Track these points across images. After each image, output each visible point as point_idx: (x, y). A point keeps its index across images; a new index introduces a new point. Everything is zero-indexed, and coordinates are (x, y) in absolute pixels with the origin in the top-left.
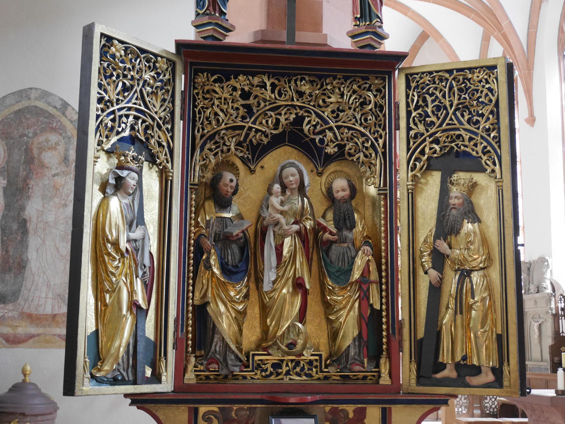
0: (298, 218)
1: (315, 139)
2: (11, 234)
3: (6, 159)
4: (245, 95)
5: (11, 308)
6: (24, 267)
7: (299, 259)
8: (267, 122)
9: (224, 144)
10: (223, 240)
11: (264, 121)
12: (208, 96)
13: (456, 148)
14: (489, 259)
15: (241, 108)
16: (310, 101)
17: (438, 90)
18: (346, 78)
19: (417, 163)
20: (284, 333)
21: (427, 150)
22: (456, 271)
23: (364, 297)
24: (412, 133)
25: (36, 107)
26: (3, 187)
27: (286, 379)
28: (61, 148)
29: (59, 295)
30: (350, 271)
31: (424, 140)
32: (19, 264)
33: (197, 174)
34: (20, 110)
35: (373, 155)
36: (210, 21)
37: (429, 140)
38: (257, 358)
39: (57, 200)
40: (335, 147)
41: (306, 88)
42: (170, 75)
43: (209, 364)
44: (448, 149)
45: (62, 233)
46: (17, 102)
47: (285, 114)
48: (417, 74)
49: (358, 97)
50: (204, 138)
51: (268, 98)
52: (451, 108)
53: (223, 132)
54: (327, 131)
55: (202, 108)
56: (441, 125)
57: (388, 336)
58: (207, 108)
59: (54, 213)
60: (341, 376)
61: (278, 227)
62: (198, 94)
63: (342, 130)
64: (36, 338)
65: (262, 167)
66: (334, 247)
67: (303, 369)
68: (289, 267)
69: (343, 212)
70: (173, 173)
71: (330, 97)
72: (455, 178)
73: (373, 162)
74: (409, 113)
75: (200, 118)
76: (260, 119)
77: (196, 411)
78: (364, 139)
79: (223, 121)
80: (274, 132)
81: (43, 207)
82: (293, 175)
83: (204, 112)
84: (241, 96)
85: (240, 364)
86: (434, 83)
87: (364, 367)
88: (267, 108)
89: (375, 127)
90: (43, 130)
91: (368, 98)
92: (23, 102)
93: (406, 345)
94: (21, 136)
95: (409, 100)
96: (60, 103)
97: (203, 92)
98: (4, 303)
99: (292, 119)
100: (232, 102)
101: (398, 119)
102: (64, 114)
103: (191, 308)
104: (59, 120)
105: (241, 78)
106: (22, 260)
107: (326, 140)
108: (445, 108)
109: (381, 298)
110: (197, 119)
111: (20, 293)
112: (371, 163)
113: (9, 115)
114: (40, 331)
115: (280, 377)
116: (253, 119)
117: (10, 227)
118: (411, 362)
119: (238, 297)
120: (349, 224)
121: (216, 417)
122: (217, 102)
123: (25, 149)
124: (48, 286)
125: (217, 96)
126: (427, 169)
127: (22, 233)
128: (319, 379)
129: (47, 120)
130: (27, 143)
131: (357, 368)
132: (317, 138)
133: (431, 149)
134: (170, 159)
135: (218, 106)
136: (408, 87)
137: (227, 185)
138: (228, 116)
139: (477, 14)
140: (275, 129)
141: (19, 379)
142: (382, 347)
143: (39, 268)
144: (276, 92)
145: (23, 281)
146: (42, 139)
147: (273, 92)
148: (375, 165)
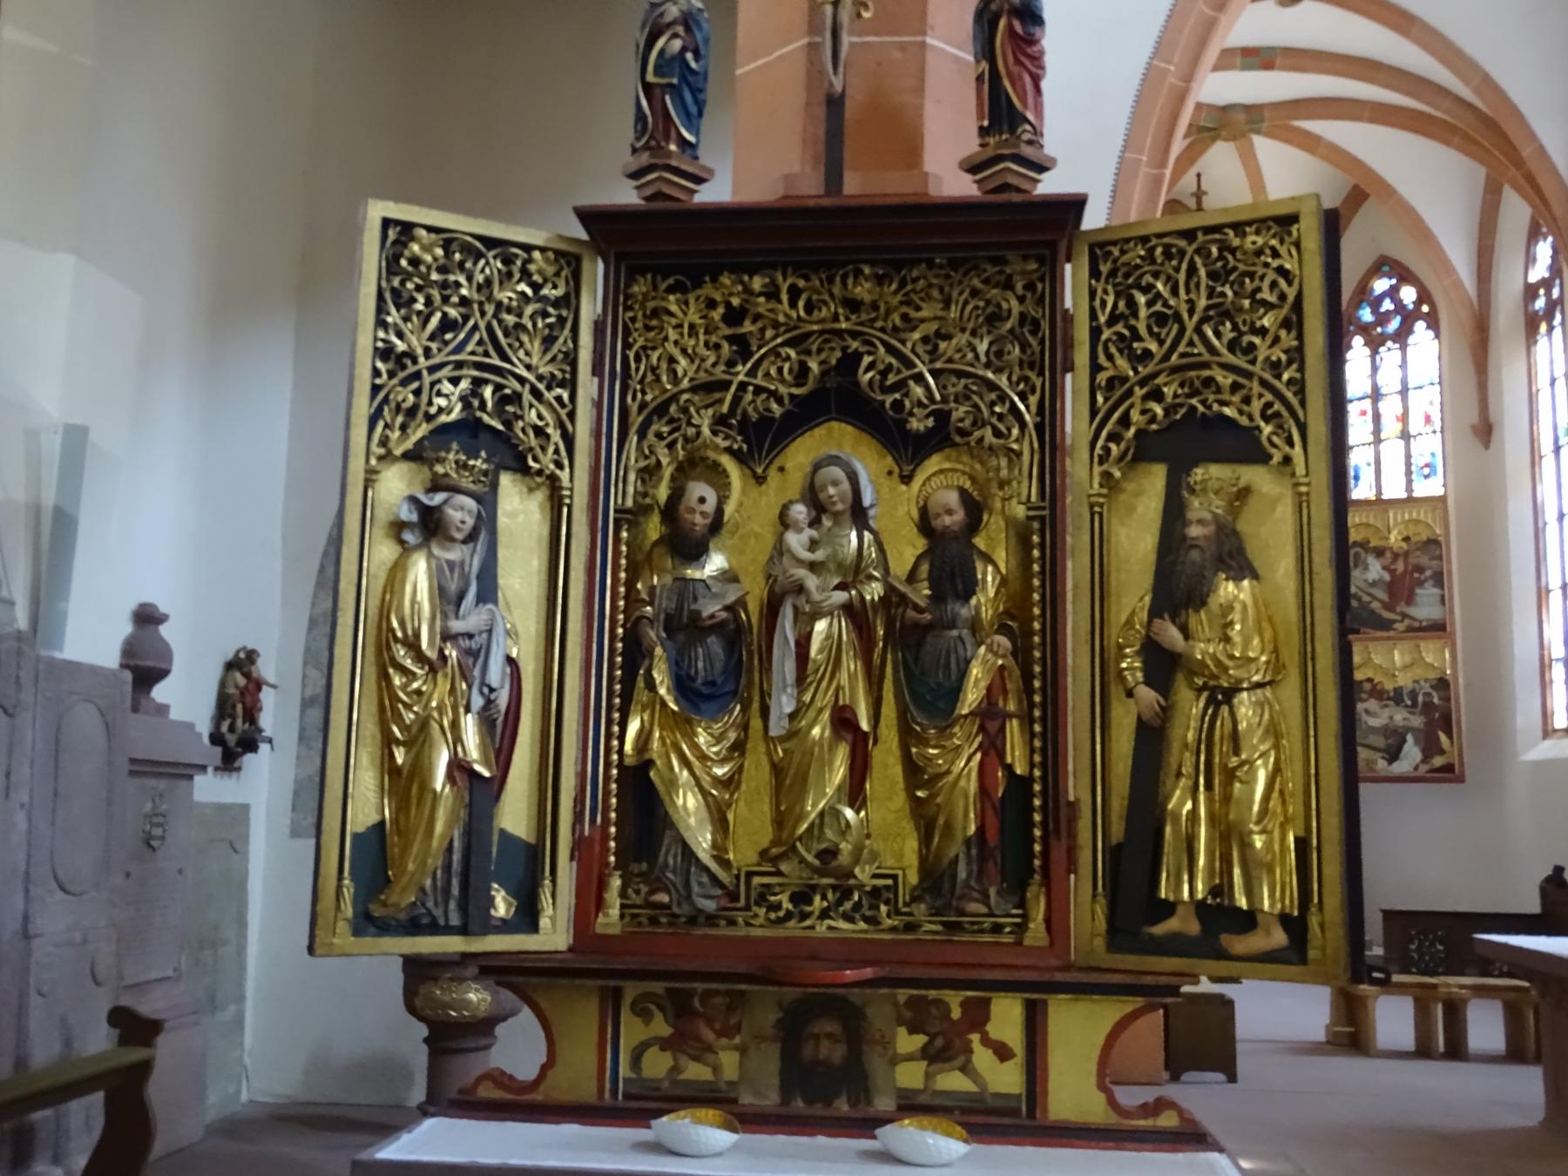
0: (850, 579)
1: (883, 402)
4: (734, 316)
7: (851, 664)
8: (780, 370)
9: (689, 424)
10: (684, 626)
11: (773, 371)
12: (654, 323)
13: (1201, 408)
14: (1276, 665)
15: (726, 346)
16: (874, 320)
17: (1163, 277)
18: (954, 264)
19: (1113, 447)
20: (812, 825)
21: (1135, 416)
22: (1200, 690)
23: (993, 748)
24: (1102, 378)
27: (821, 929)
30: (956, 692)
31: (1130, 393)
33: (631, 490)
35: (1015, 432)
36: (653, 161)
37: (1139, 392)
38: (757, 880)
40: (927, 416)
41: (863, 290)
42: (567, 283)
43: (653, 892)
44: (1183, 411)
47: (820, 351)
48: (1114, 243)
49: (982, 304)
50: (646, 412)
51: (781, 319)
52: (1191, 316)
53: (685, 396)
54: (911, 383)
55: (644, 348)
56: (1166, 358)
57: (1045, 840)
58: (654, 349)
60: (942, 923)
61: (803, 598)
62: (633, 320)
63: (942, 380)
65: (781, 469)
66: (929, 639)
67: (857, 906)
68: (824, 684)
69: (949, 558)
70: (571, 489)
71: (918, 309)
72: (1199, 478)
73: (1015, 446)
74: (1095, 332)
75: (637, 369)
76: (765, 364)
77: (617, 995)
78: (993, 396)
79: (685, 374)
80: (795, 391)
82: (835, 483)
83: (648, 357)
84: (725, 318)
85: (719, 892)
86: (1153, 261)
87: (988, 906)
88: (779, 340)
89: (1021, 368)
91: (1005, 305)
93: (1085, 857)
95: (1097, 303)
97: (644, 315)
99: (834, 362)
100: (707, 332)
101: (1069, 346)
103: (615, 772)
105: (726, 280)
107: (907, 403)
108: (1177, 317)
109: (1032, 751)
110: (633, 372)
112: (1012, 450)
115: (808, 923)
116: (749, 365)
118: (1094, 896)
119: (714, 749)
120: (960, 586)
121: (661, 1008)
122: (673, 335)
125: (674, 321)
126: (1135, 459)
128: (893, 929)
131: (975, 907)
132: (889, 400)
133: (1143, 412)
134: (566, 462)
135: (676, 343)
136: (1095, 273)
137: (693, 511)
138: (697, 362)
139: (1466, 137)
140: (798, 385)
142: (1032, 863)
144: (801, 304)
147: (793, 304)
148: (1019, 454)
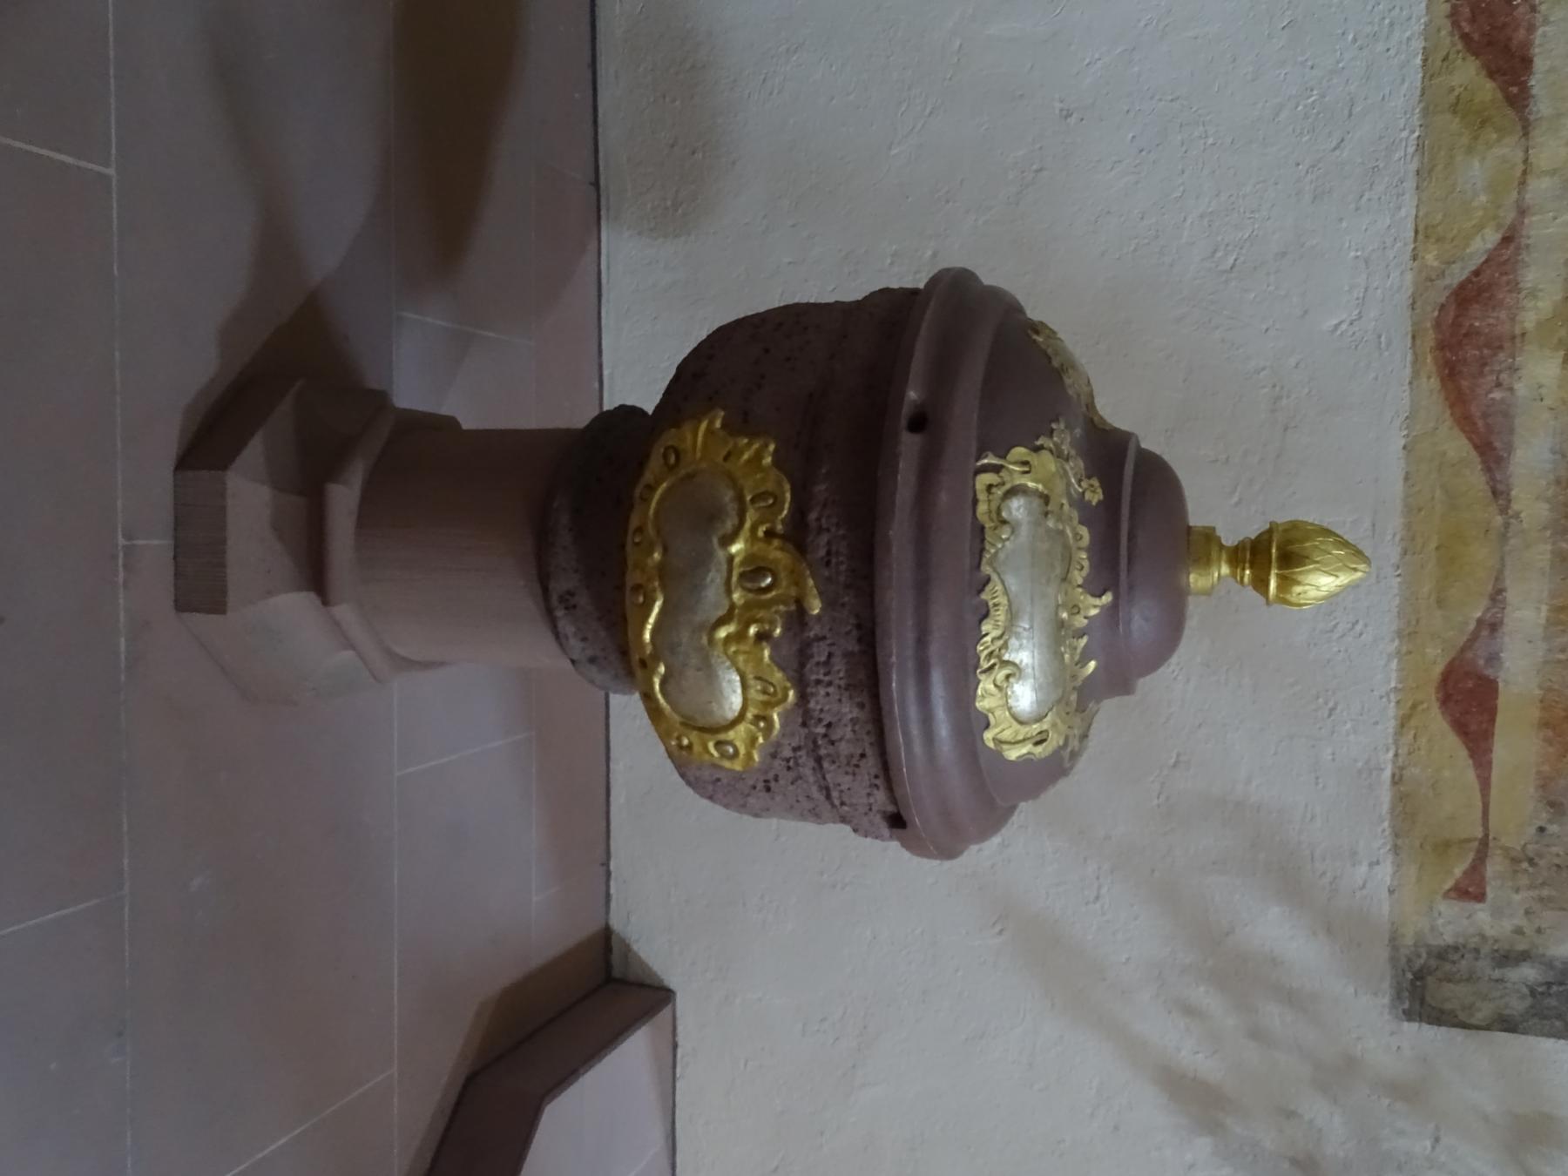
64: (1475, 479)
114: (1531, 501)
141: (1218, 503)
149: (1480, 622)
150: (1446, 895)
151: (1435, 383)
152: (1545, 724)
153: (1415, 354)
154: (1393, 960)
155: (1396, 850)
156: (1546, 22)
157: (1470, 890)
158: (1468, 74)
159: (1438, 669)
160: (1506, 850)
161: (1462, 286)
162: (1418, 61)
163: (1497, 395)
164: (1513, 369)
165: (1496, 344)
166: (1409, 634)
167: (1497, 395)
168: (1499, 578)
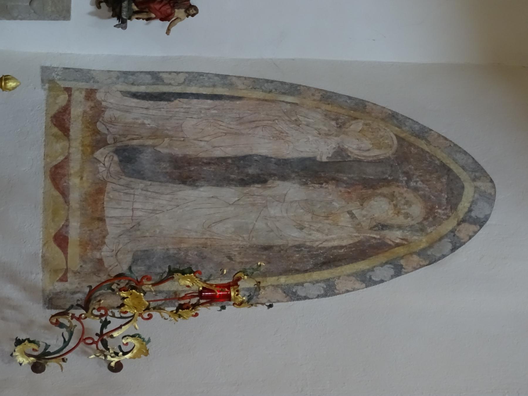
2: (238, 168)
3: (363, 158)
5: (112, 169)
6: (184, 182)
25: (463, 187)
26: (315, 157)
28: (400, 220)
29: (139, 224)
32: (189, 177)
34: (449, 170)
39: (308, 217)
45: (251, 227)
46: (463, 168)
59: (285, 215)
64: (61, 199)
81: (291, 202)
90: (425, 198)
92: (465, 173)
94: (406, 173)
96: (481, 216)
98: (121, 161)
102: (463, 221)
104: (449, 217)
106: (195, 181)
111: (139, 178)
113: (439, 159)
117: (250, 166)
123: (386, 179)
124: (154, 211)
127: (242, 180)
129: (444, 201)
130: (397, 180)
143: (185, 199)
145: (160, 182)
146: (410, 196)
149: (63, 225)
150: (57, 281)
151: (50, 181)
152: (80, 245)
153: (45, 177)
154: (43, 296)
155: (43, 271)
156: (72, 124)
157: (64, 279)
158: (55, 130)
159: (53, 234)
160: (73, 271)
161: (56, 165)
162: (44, 127)
163: (65, 184)
164: (69, 180)
165: (65, 175)
166: (46, 227)
167: (65, 184)
168: (68, 217)
